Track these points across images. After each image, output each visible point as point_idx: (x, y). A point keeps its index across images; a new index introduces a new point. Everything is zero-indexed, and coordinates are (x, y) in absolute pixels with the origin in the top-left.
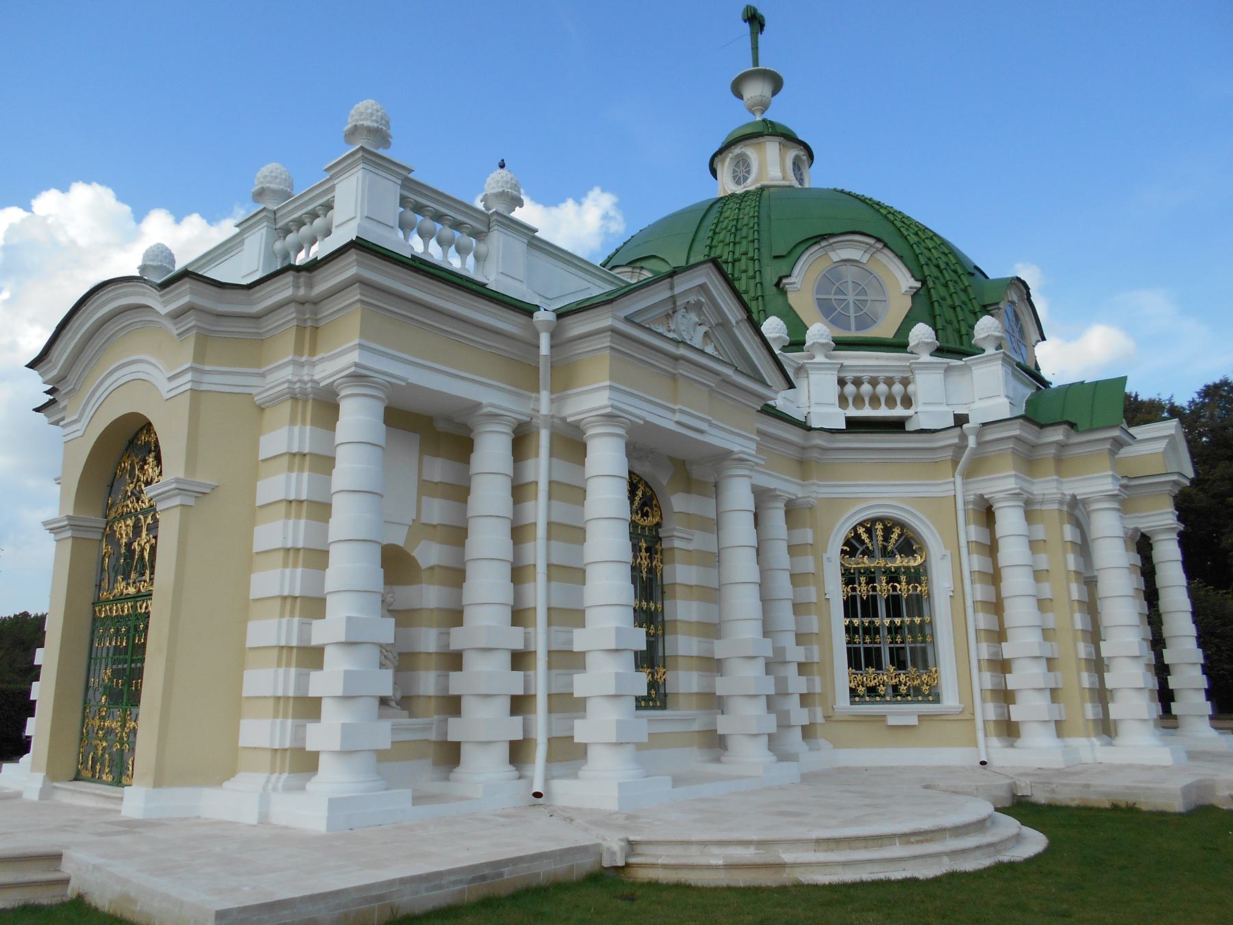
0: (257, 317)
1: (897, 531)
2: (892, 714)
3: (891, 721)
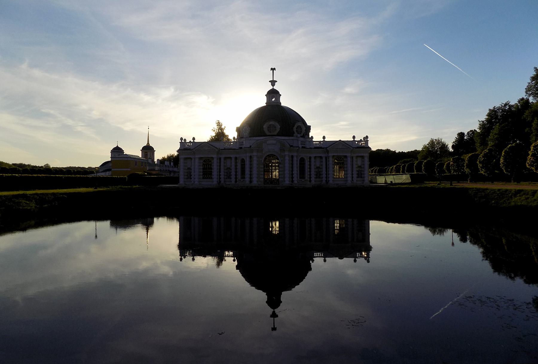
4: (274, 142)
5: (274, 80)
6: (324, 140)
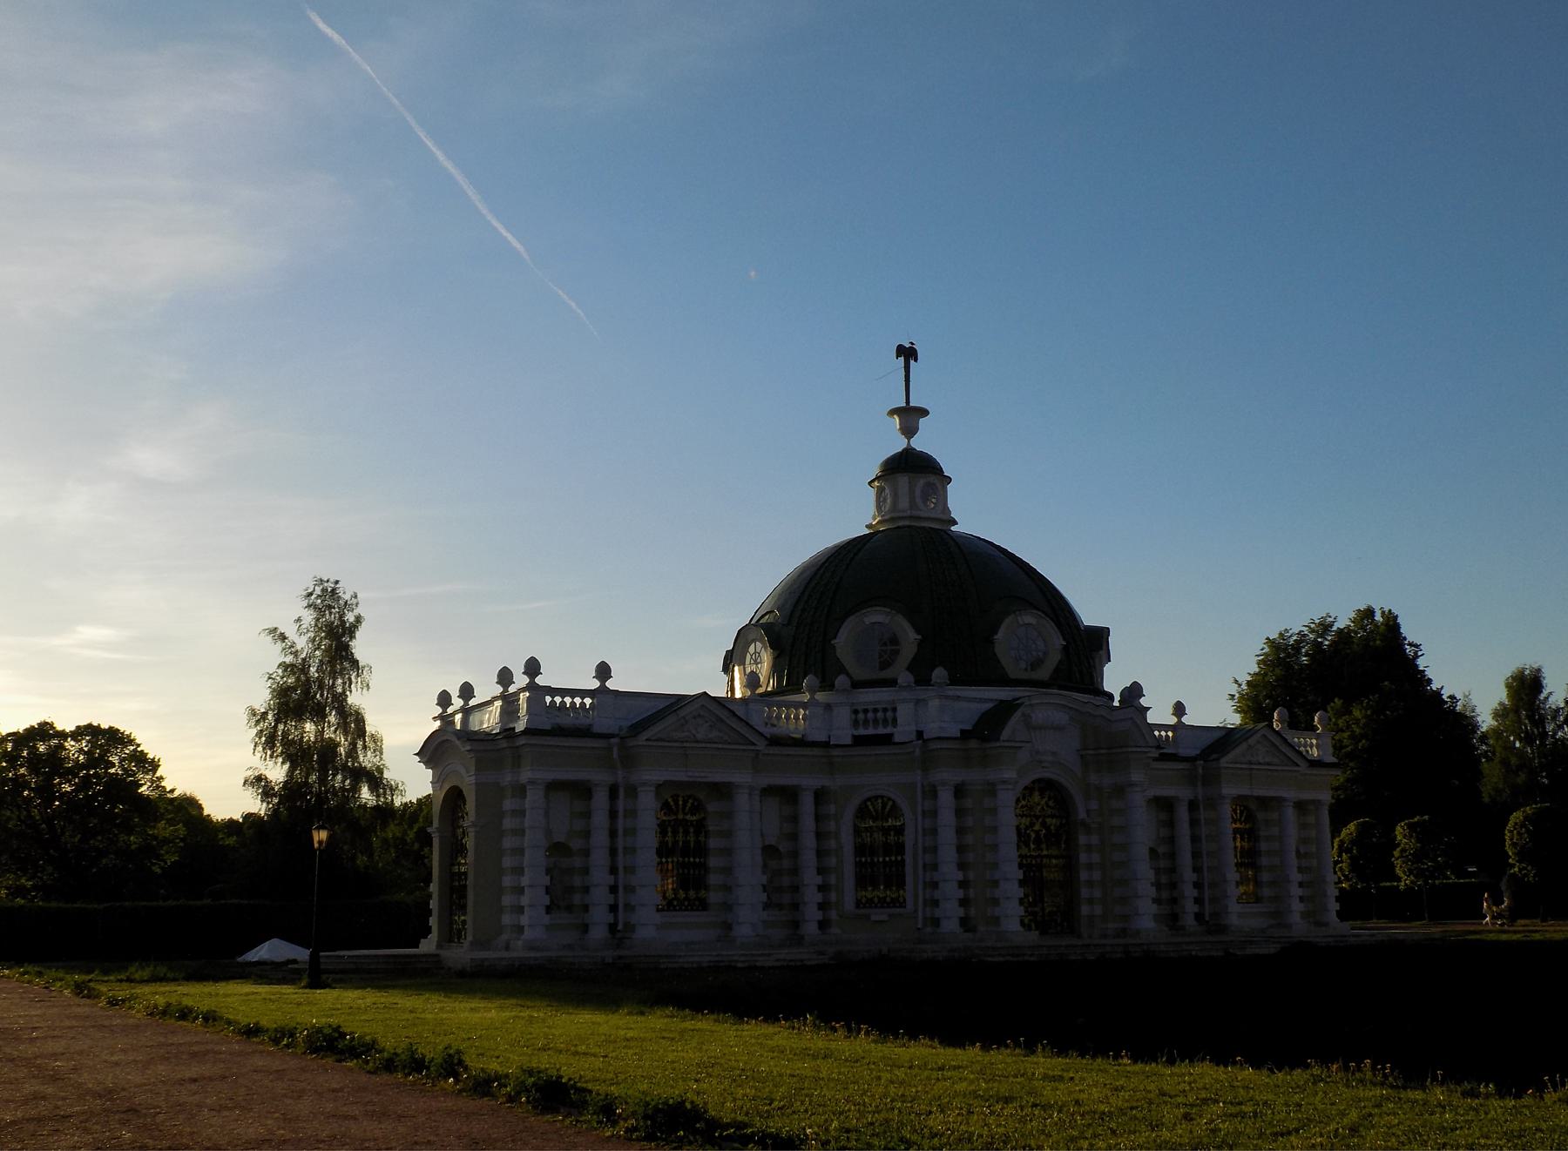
0: (498, 750)
1: (890, 803)
3: (874, 918)
4: (1061, 717)
6: (1180, 721)
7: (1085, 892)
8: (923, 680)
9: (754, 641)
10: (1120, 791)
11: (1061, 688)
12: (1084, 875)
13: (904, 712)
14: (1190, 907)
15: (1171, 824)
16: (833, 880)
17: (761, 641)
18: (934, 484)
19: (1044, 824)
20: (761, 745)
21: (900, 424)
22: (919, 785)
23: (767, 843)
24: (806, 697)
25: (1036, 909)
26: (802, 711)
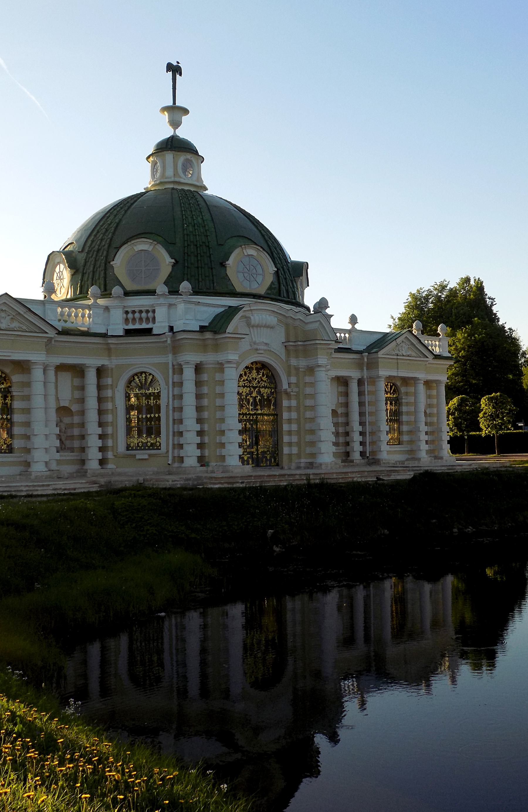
1: (151, 377)
2: (139, 454)
3: (138, 457)
5: (177, 104)
6: (353, 327)
7: (286, 439)
8: (174, 291)
9: (59, 263)
10: (311, 370)
11: (272, 299)
12: (286, 427)
13: (161, 313)
14: (357, 448)
15: (346, 394)
16: (110, 430)
17: (64, 265)
18: (191, 161)
19: (259, 392)
20: (52, 333)
21: (169, 119)
22: (170, 366)
23: (62, 404)
24: (90, 302)
25: (252, 450)
26: (87, 312)
